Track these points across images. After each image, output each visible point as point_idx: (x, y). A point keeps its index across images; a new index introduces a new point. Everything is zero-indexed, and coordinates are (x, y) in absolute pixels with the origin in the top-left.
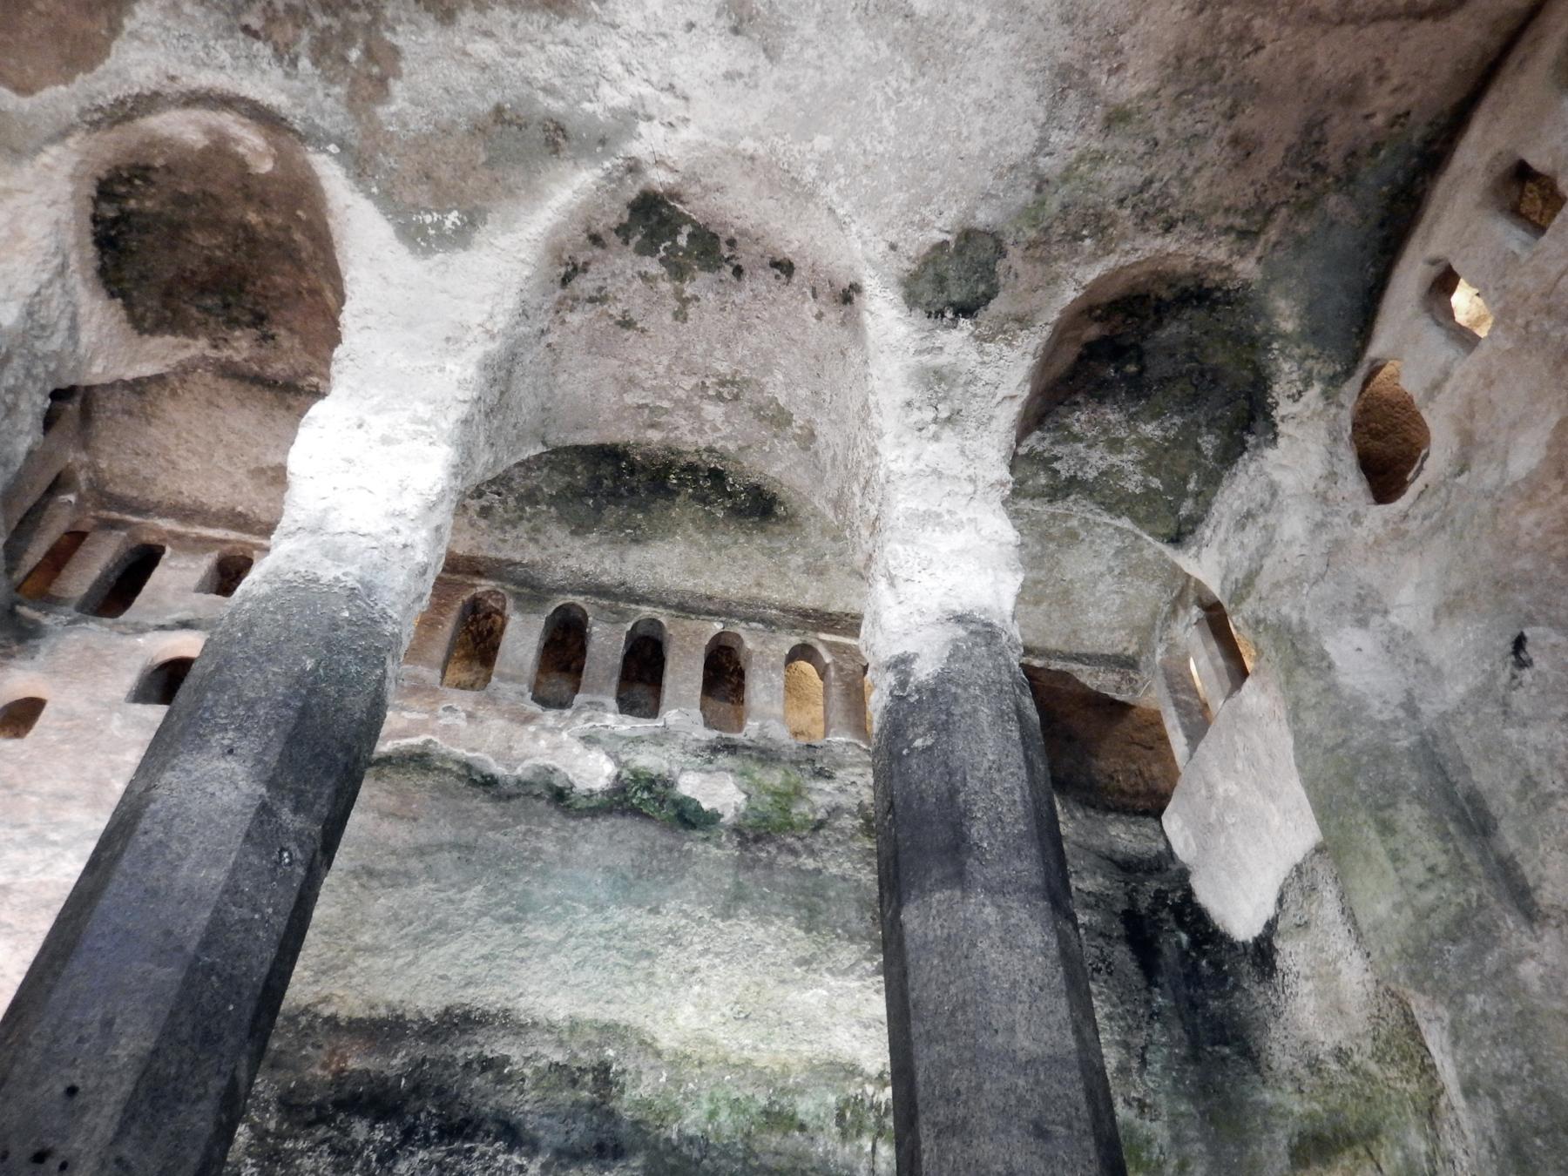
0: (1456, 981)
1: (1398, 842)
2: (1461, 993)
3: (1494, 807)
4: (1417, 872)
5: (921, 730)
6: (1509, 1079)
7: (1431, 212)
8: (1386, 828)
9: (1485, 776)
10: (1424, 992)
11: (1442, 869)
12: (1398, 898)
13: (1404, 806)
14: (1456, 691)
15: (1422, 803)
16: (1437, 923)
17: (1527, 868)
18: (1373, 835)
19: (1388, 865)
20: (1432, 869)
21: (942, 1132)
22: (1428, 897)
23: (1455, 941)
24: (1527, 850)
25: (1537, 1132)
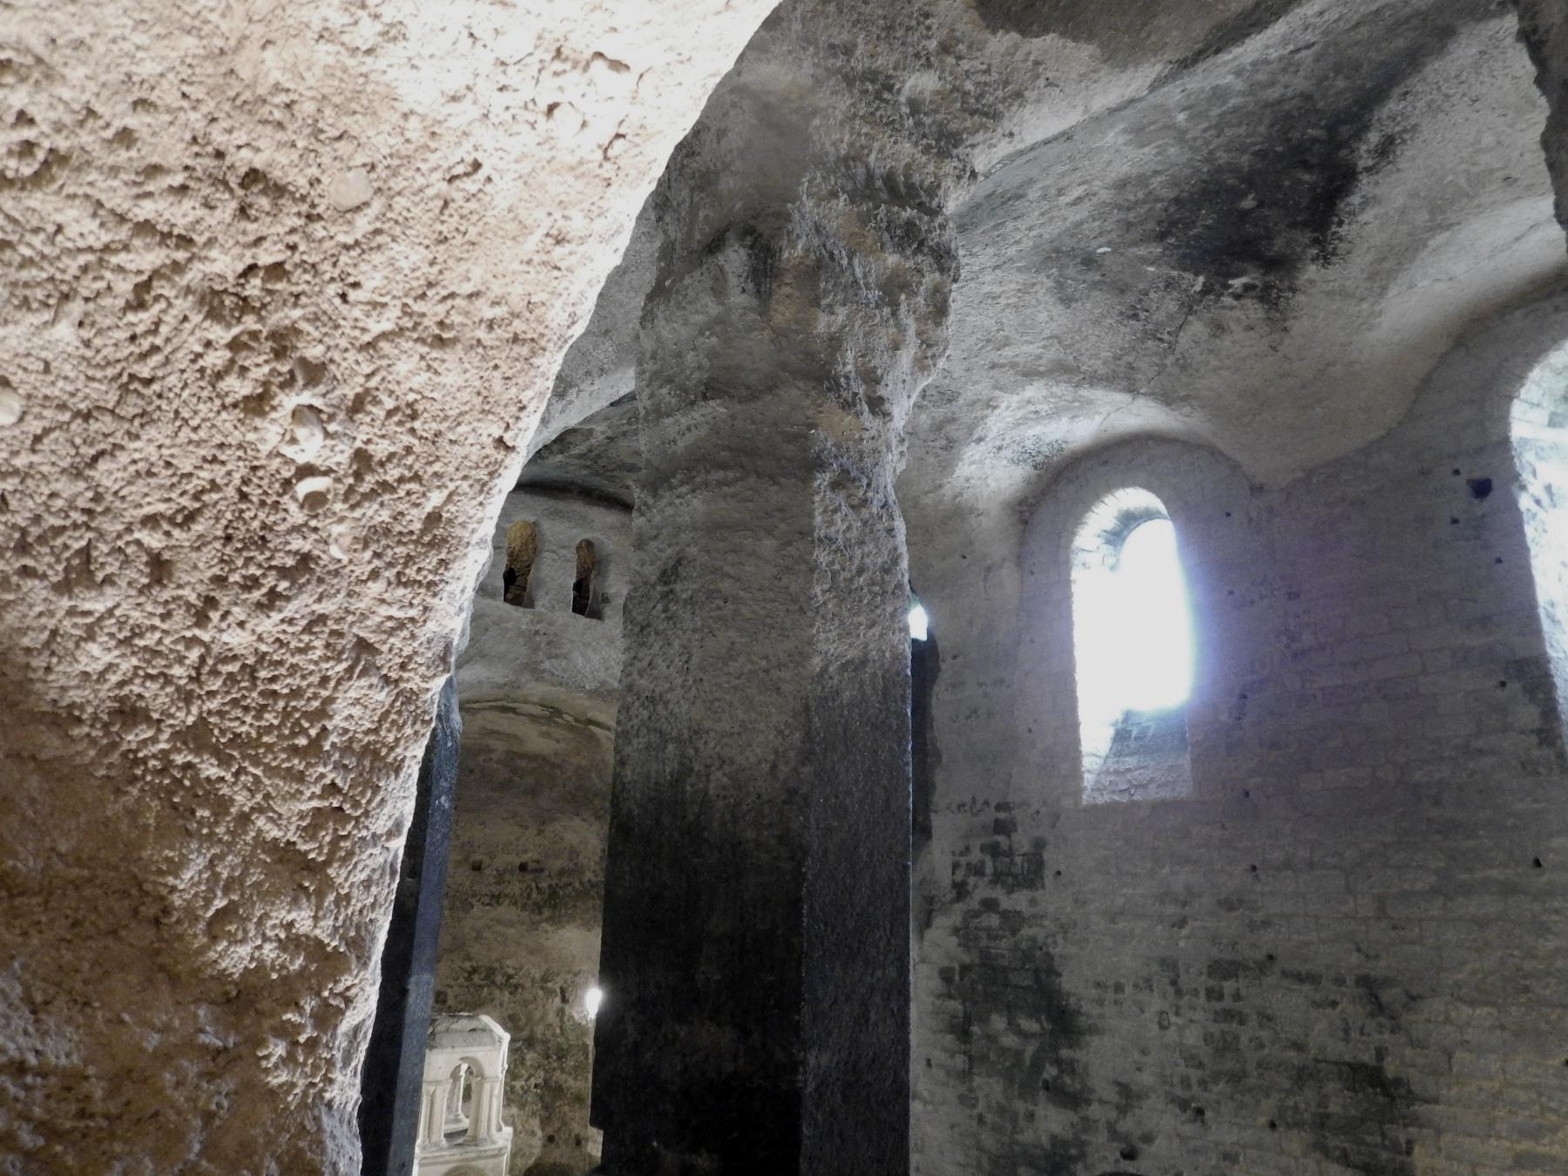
7: (561, 505)
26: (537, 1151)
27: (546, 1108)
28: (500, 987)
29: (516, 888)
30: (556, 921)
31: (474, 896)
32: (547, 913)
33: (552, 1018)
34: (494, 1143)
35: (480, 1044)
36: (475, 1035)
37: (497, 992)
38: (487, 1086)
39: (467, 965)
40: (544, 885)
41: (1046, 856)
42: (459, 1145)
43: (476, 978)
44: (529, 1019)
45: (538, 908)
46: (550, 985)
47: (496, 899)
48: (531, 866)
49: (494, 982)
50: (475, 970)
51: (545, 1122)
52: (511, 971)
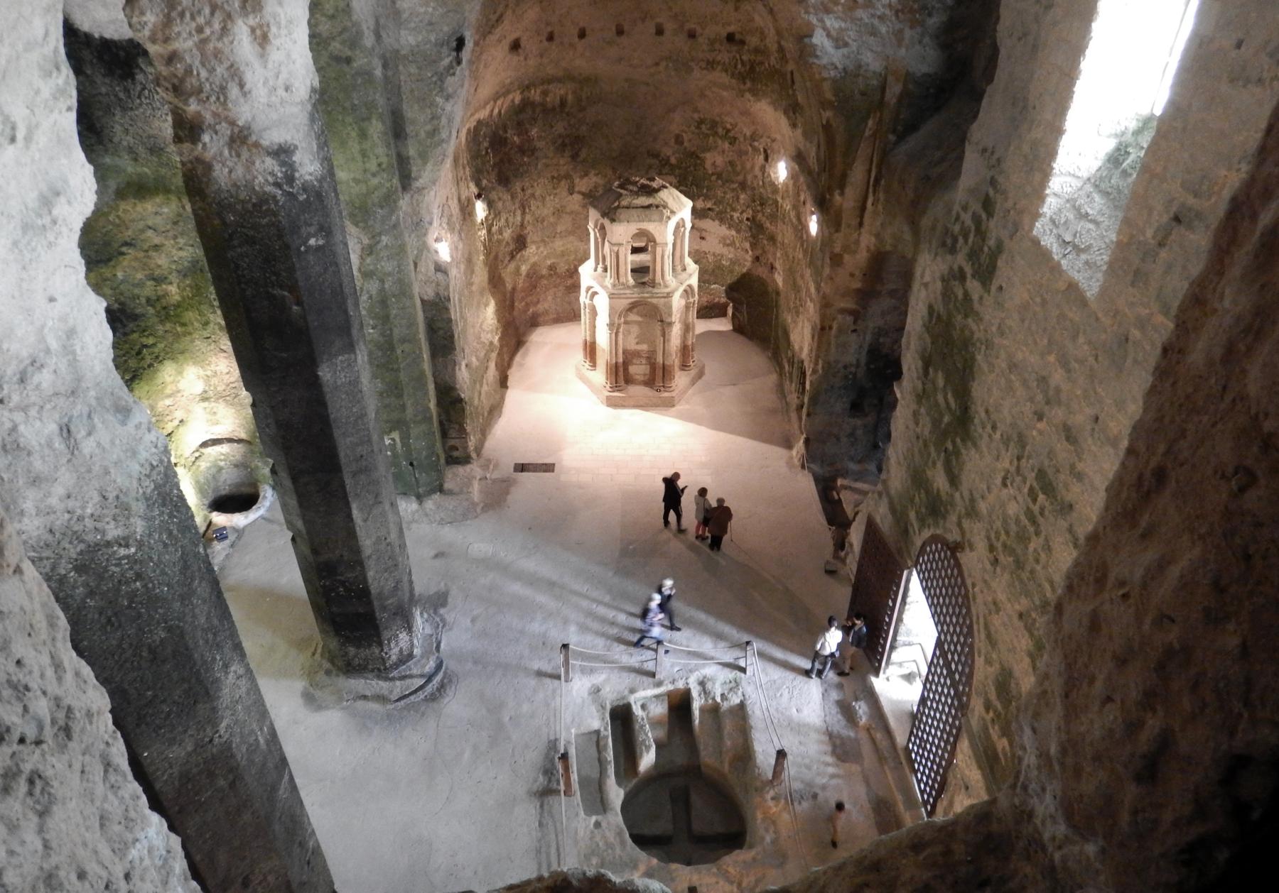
0: (378, 228)
1: (367, 145)
2: (380, 234)
3: (409, 129)
4: (372, 166)
5: (312, 230)
6: (389, 274)
8: (363, 135)
9: (411, 112)
10: (356, 225)
11: (384, 166)
12: (358, 177)
13: (374, 122)
14: (408, 39)
15: (384, 123)
16: (376, 197)
17: (414, 169)
18: (354, 134)
19: (359, 158)
20: (379, 165)
21: (354, 474)
22: (375, 181)
23: (382, 207)
24: (419, 162)
25: (394, 296)
26: (748, 264)
27: (753, 236)
28: (721, 138)
29: (724, 57)
30: (754, 92)
31: (693, 60)
32: (749, 84)
33: (757, 171)
34: (666, 286)
35: (650, 221)
36: (648, 212)
37: (720, 142)
38: (659, 250)
39: (696, 116)
40: (745, 58)
41: (1000, 263)
42: (644, 283)
43: (703, 127)
44: (743, 168)
45: (742, 78)
46: (756, 144)
47: (711, 65)
48: (738, 37)
49: (716, 133)
50: (701, 122)
51: (753, 246)
52: (729, 126)
